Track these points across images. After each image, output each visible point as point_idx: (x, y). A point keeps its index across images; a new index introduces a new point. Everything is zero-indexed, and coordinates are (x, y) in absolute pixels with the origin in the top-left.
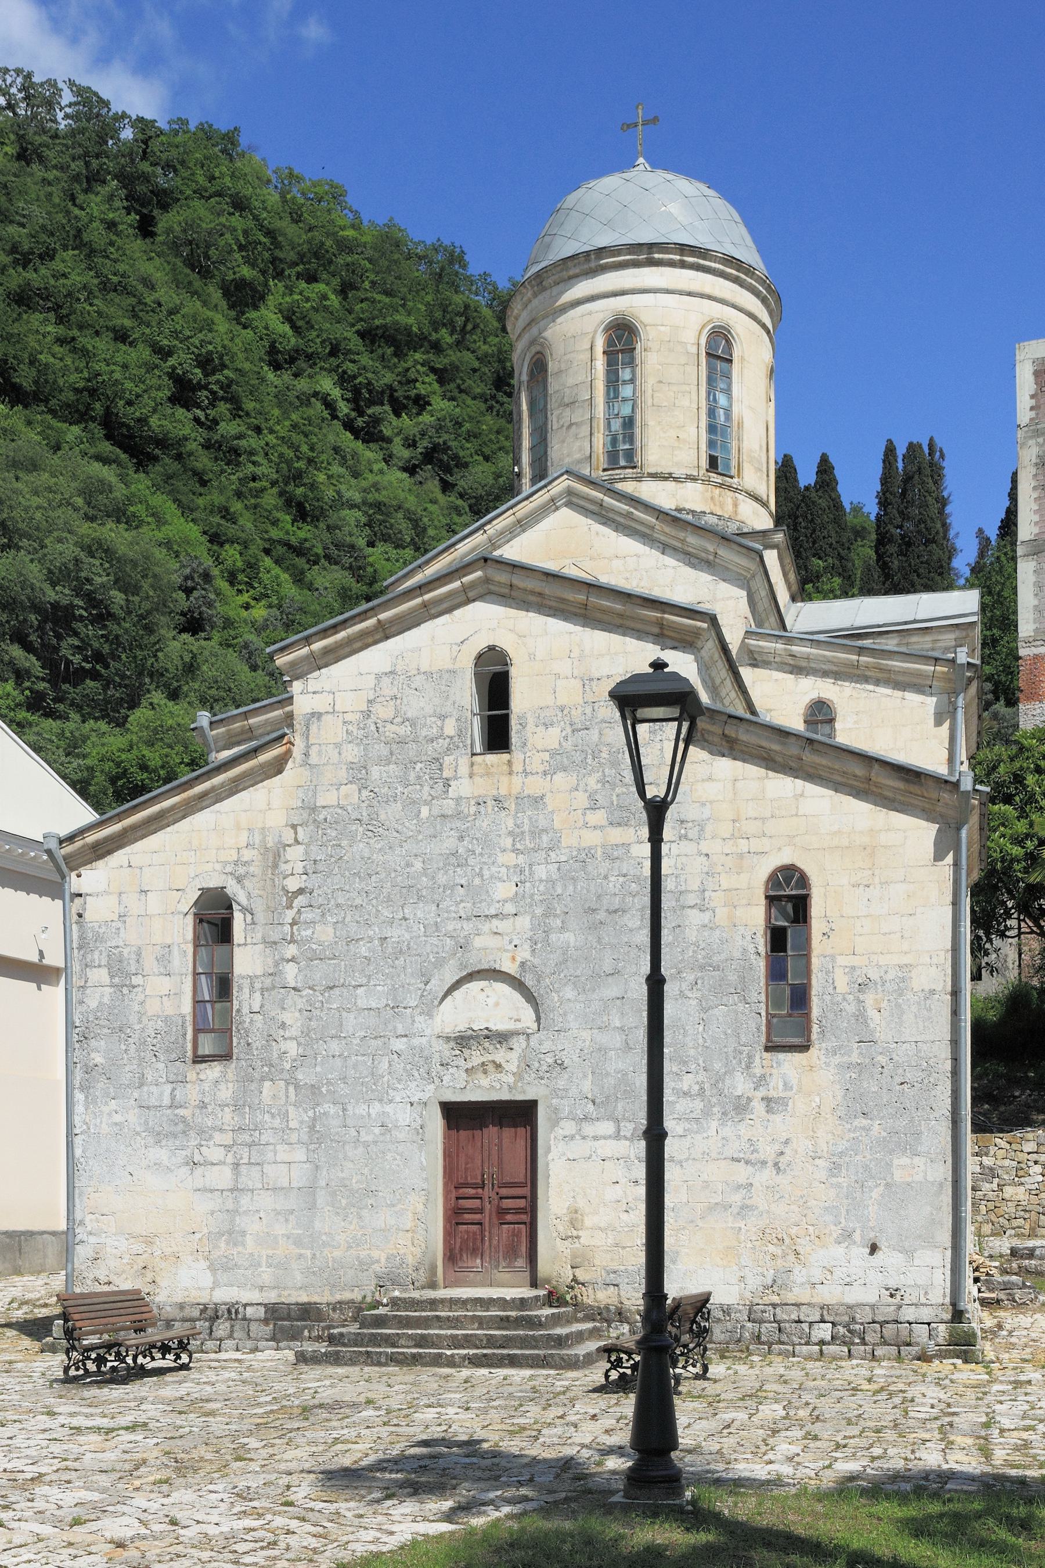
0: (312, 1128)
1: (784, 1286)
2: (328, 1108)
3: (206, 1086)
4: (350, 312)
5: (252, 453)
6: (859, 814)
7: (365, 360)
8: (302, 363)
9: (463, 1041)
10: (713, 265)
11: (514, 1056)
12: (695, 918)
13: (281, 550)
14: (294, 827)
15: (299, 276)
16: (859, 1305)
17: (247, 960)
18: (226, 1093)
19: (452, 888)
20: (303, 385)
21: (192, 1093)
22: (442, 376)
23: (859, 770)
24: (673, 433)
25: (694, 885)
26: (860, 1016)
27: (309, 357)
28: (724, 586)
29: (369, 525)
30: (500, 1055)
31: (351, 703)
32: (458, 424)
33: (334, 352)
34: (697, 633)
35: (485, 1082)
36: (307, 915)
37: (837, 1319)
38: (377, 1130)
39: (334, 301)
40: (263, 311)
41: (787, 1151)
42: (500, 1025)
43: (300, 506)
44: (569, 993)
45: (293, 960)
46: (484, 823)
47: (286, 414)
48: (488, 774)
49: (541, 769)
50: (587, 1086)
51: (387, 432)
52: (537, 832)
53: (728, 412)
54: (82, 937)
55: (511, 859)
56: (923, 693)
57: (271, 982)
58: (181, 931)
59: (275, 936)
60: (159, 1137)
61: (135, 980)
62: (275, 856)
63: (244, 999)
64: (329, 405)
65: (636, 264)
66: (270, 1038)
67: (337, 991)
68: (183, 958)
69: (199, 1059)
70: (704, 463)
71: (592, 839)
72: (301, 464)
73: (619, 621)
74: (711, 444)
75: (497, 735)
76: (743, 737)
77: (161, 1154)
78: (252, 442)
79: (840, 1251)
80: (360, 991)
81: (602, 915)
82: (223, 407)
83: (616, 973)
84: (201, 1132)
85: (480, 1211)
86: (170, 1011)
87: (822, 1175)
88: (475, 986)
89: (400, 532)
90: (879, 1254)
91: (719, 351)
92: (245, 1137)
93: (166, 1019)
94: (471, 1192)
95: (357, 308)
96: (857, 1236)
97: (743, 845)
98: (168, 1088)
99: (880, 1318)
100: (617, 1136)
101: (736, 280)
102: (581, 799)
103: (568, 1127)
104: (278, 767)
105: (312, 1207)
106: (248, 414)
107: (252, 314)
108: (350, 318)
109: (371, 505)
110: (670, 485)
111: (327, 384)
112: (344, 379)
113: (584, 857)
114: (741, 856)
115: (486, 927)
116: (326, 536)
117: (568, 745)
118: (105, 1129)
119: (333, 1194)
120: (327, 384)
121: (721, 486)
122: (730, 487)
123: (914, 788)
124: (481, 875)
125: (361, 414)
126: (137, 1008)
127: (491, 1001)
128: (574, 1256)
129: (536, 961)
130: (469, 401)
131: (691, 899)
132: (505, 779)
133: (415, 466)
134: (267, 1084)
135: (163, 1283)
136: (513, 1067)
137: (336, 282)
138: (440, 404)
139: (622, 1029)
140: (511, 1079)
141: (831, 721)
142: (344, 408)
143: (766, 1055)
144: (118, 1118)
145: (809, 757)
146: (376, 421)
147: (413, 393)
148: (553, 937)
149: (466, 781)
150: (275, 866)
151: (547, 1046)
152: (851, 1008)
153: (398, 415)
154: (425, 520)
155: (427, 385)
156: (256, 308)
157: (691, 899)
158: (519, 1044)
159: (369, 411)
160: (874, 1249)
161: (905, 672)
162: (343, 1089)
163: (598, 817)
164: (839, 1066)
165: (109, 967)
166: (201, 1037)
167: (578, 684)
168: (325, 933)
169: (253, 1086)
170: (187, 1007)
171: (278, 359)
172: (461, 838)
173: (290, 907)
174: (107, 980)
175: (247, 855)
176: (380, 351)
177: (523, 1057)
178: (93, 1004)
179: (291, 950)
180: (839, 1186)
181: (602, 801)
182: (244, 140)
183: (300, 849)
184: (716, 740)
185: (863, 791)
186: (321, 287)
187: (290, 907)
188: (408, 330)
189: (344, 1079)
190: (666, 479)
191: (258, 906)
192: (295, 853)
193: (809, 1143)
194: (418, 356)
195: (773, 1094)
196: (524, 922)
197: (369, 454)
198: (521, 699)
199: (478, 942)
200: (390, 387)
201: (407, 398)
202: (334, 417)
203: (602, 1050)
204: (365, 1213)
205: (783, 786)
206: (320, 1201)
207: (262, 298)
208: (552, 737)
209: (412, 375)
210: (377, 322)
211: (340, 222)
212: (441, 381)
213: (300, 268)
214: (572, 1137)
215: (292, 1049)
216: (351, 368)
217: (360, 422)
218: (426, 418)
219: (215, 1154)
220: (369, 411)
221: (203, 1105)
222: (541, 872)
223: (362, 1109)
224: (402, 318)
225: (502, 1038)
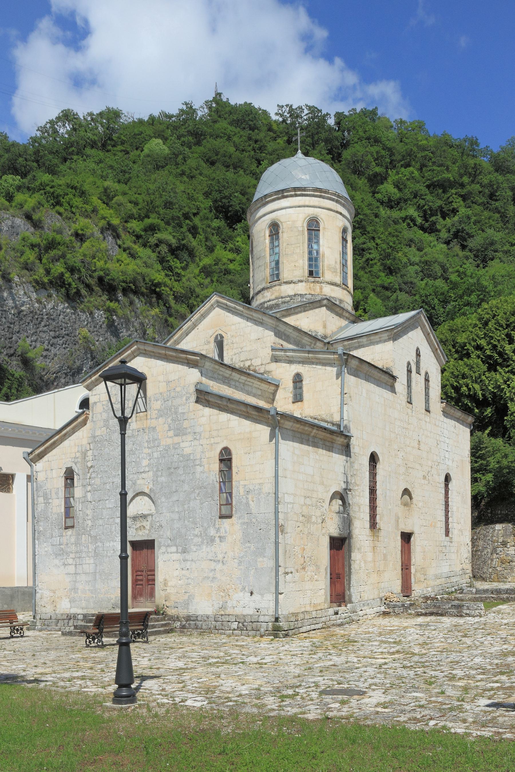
0: (95, 551)
1: (225, 608)
2: (99, 544)
3: (68, 537)
4: (423, 177)
5: (370, 249)
6: (246, 425)
7: (429, 197)
8: (402, 204)
10: (308, 193)
11: (148, 523)
12: (199, 469)
13: (379, 289)
14: (89, 444)
15: (402, 166)
16: (247, 615)
18: (73, 540)
19: (131, 463)
20: (403, 214)
21: (64, 540)
23: (243, 408)
24: (293, 264)
25: (198, 457)
26: (247, 504)
27: (406, 201)
28: (267, 331)
29: (422, 271)
30: (145, 523)
33: (415, 197)
34: (197, 361)
35: (140, 533)
36: (93, 475)
37: (240, 621)
38: (112, 552)
39: (416, 173)
40: (385, 184)
41: (226, 556)
42: (146, 512)
43: (389, 268)
44: (163, 499)
45: (90, 491)
46: (139, 438)
47: (386, 230)
48: (141, 420)
49: (155, 416)
50: (169, 534)
51: (439, 227)
52: (154, 440)
53: (318, 252)
54: (37, 487)
55: (146, 451)
56: (332, 366)
59: (85, 484)
61: (50, 501)
62: (84, 454)
64: (413, 220)
65: (278, 199)
66: (84, 520)
67: (101, 502)
69: (66, 528)
70: (307, 273)
71: (169, 441)
72: (390, 251)
73: (175, 359)
74: (310, 266)
76: (211, 399)
77: (57, 562)
79: (241, 594)
80: (107, 501)
81: (172, 470)
83: (176, 491)
84: (67, 554)
85: (142, 580)
86: (59, 512)
87: (236, 565)
88: (138, 498)
89: (436, 272)
90: (253, 595)
91: (313, 227)
92: (78, 555)
93: (58, 514)
94: (140, 573)
95: (426, 174)
96: (247, 589)
97: (212, 441)
98: (58, 538)
99: (253, 620)
100: (177, 552)
101: (320, 197)
102: (166, 427)
103: (163, 549)
105: (95, 580)
106: (369, 233)
107: (381, 187)
108: (424, 180)
109: (423, 263)
110: (292, 285)
111: (412, 211)
112: (419, 208)
113: (167, 449)
114: (212, 444)
115: (140, 476)
116: (400, 280)
117: (163, 407)
118: (43, 553)
119: (101, 575)
120: (412, 211)
121: (314, 282)
122: (318, 282)
123: (261, 414)
124: (139, 457)
125: (427, 221)
126: (50, 510)
127: (143, 503)
128: (166, 597)
129: (154, 488)
131: (198, 462)
132: (145, 421)
133: (449, 241)
134: (83, 536)
135: (58, 606)
136: (148, 527)
137: (418, 165)
138: (463, 211)
139: (178, 512)
140: (147, 532)
141: (302, 381)
142: (419, 221)
143: (220, 520)
144: (46, 549)
145: (230, 406)
146: (434, 223)
147: (451, 208)
148: (159, 479)
149: (135, 423)
150: (85, 458)
151: (158, 519)
152: (244, 501)
153: (444, 219)
154: (448, 265)
155: (458, 203)
156: (382, 183)
157: (198, 462)
158: (149, 518)
159: (431, 220)
160: (252, 593)
161: (325, 359)
162: (103, 537)
163: (171, 434)
164: (241, 523)
165: (43, 496)
166: (67, 520)
167: (165, 384)
168: (97, 481)
169: (80, 537)
170: (63, 510)
171: (391, 204)
172: (133, 444)
173: (89, 473)
174: (43, 501)
175: (78, 455)
176: (436, 192)
177: (151, 524)
178: (40, 510)
179: (89, 488)
180: (241, 569)
181: (172, 427)
182: (379, 112)
183: (91, 451)
184: (204, 401)
185: (247, 416)
186: (411, 169)
187: (89, 473)
188: (449, 180)
189: (103, 533)
190: (290, 283)
191: (80, 473)
192: (90, 453)
193: (232, 553)
194: (453, 191)
195: (222, 535)
196: (151, 474)
197: (431, 239)
199: (139, 482)
200: (441, 207)
201: (449, 210)
202: (415, 225)
203: (173, 520)
204: (109, 581)
205: (224, 416)
206: (97, 577)
207: (386, 179)
209: (451, 200)
210: (435, 179)
211: (420, 139)
212: (464, 200)
213: (402, 163)
214: (165, 553)
215: (89, 523)
216: (422, 202)
217: (427, 225)
218: (456, 218)
219: (70, 561)
220: (431, 220)
221: (67, 544)
222: (156, 455)
223: (108, 544)
224: (447, 175)
225: (144, 517)
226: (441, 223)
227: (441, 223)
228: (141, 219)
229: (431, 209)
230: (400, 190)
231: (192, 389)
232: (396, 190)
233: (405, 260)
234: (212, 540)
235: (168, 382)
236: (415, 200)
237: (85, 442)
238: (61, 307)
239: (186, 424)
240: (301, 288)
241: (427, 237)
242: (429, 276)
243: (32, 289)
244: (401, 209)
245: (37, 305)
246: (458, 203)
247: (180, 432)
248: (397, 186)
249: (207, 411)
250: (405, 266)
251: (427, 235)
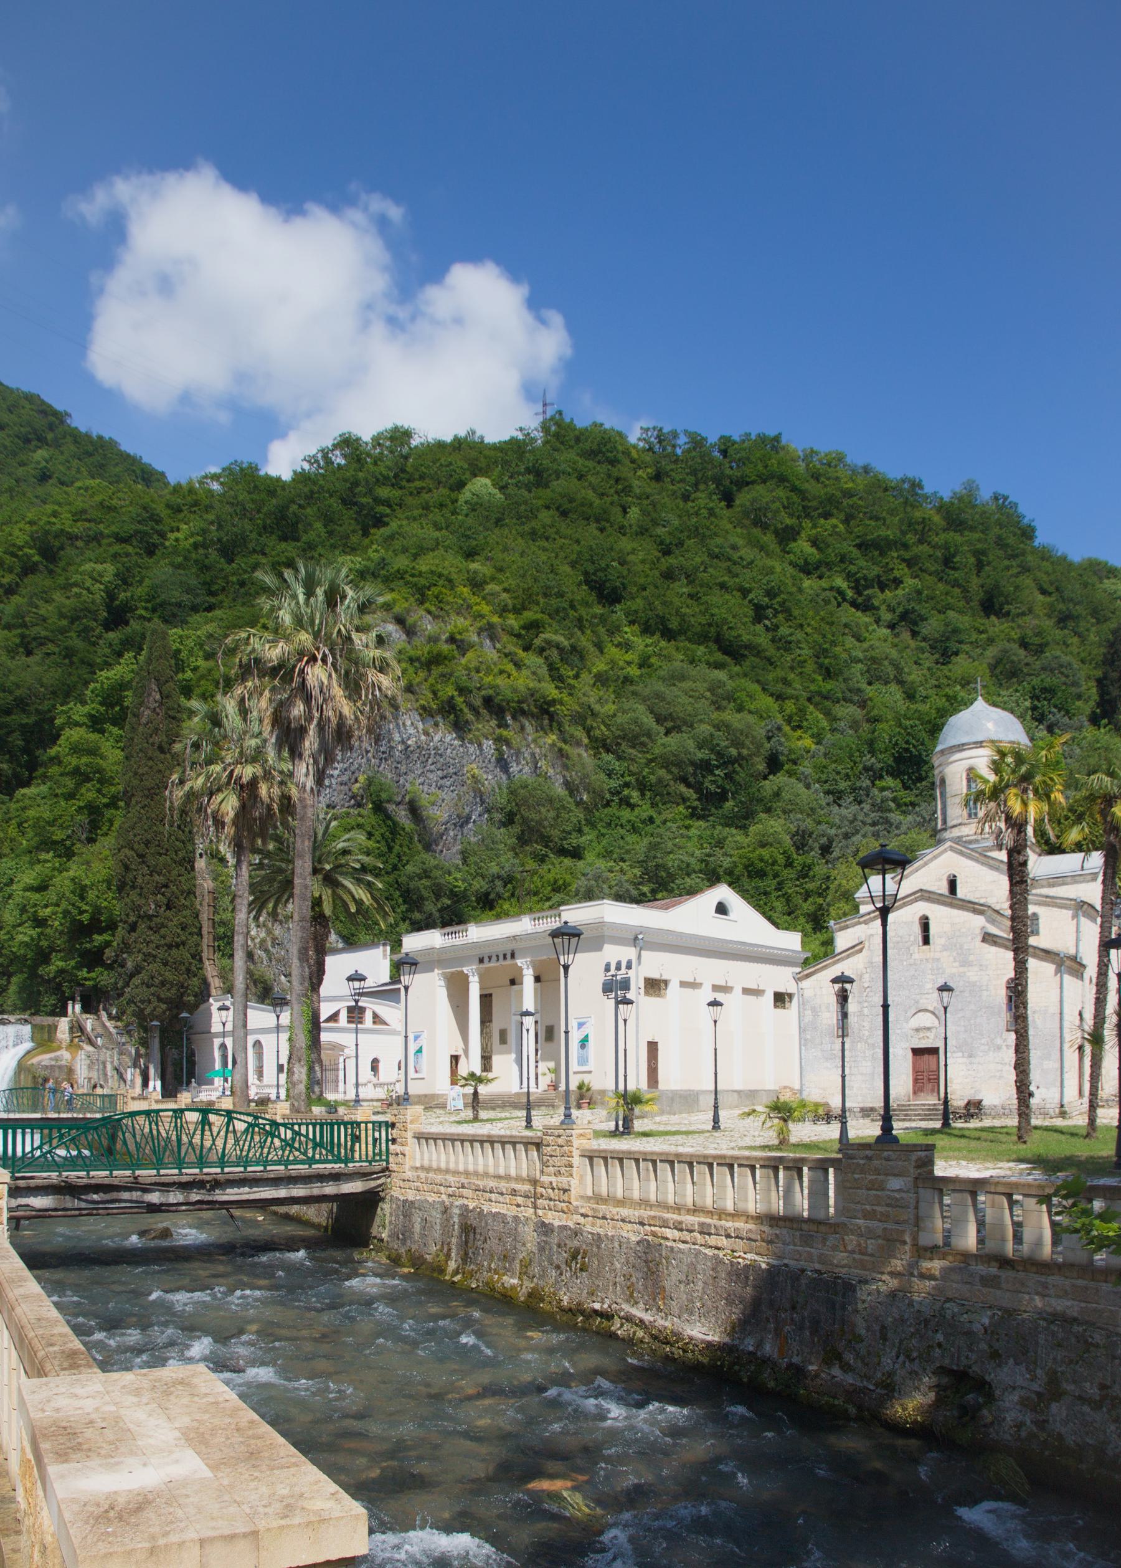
7: (862, 563)
8: (823, 569)
22: (910, 563)
27: (827, 564)
32: (919, 593)
33: (842, 561)
39: (841, 528)
47: (817, 613)
64: (840, 592)
71: (954, 970)
75: (926, 941)
78: (799, 635)
82: (781, 617)
104: (861, 950)
111: (840, 582)
112: (849, 576)
120: (840, 582)
130: (927, 577)
138: (910, 582)
142: (850, 594)
146: (869, 598)
153: (882, 591)
155: (901, 570)
156: (795, 540)
188: (886, 538)
197: (867, 619)
200: (879, 576)
202: (844, 600)
208: (943, 941)
212: (909, 566)
216: (853, 569)
218: (900, 592)
226: (879, 598)
227: (879, 598)
228: (517, 611)
229: (865, 578)
230: (819, 549)
231: (978, 931)
232: (814, 550)
233: (844, 656)
235: (953, 924)
236: (843, 566)
237: (861, 966)
238: (448, 738)
239: (971, 958)
241: (864, 619)
242: (879, 678)
243: (418, 717)
244: (820, 577)
245: (423, 738)
246: (901, 570)
247: (965, 963)
248: (814, 543)
249: (994, 949)
250: (848, 666)
251: (859, 614)
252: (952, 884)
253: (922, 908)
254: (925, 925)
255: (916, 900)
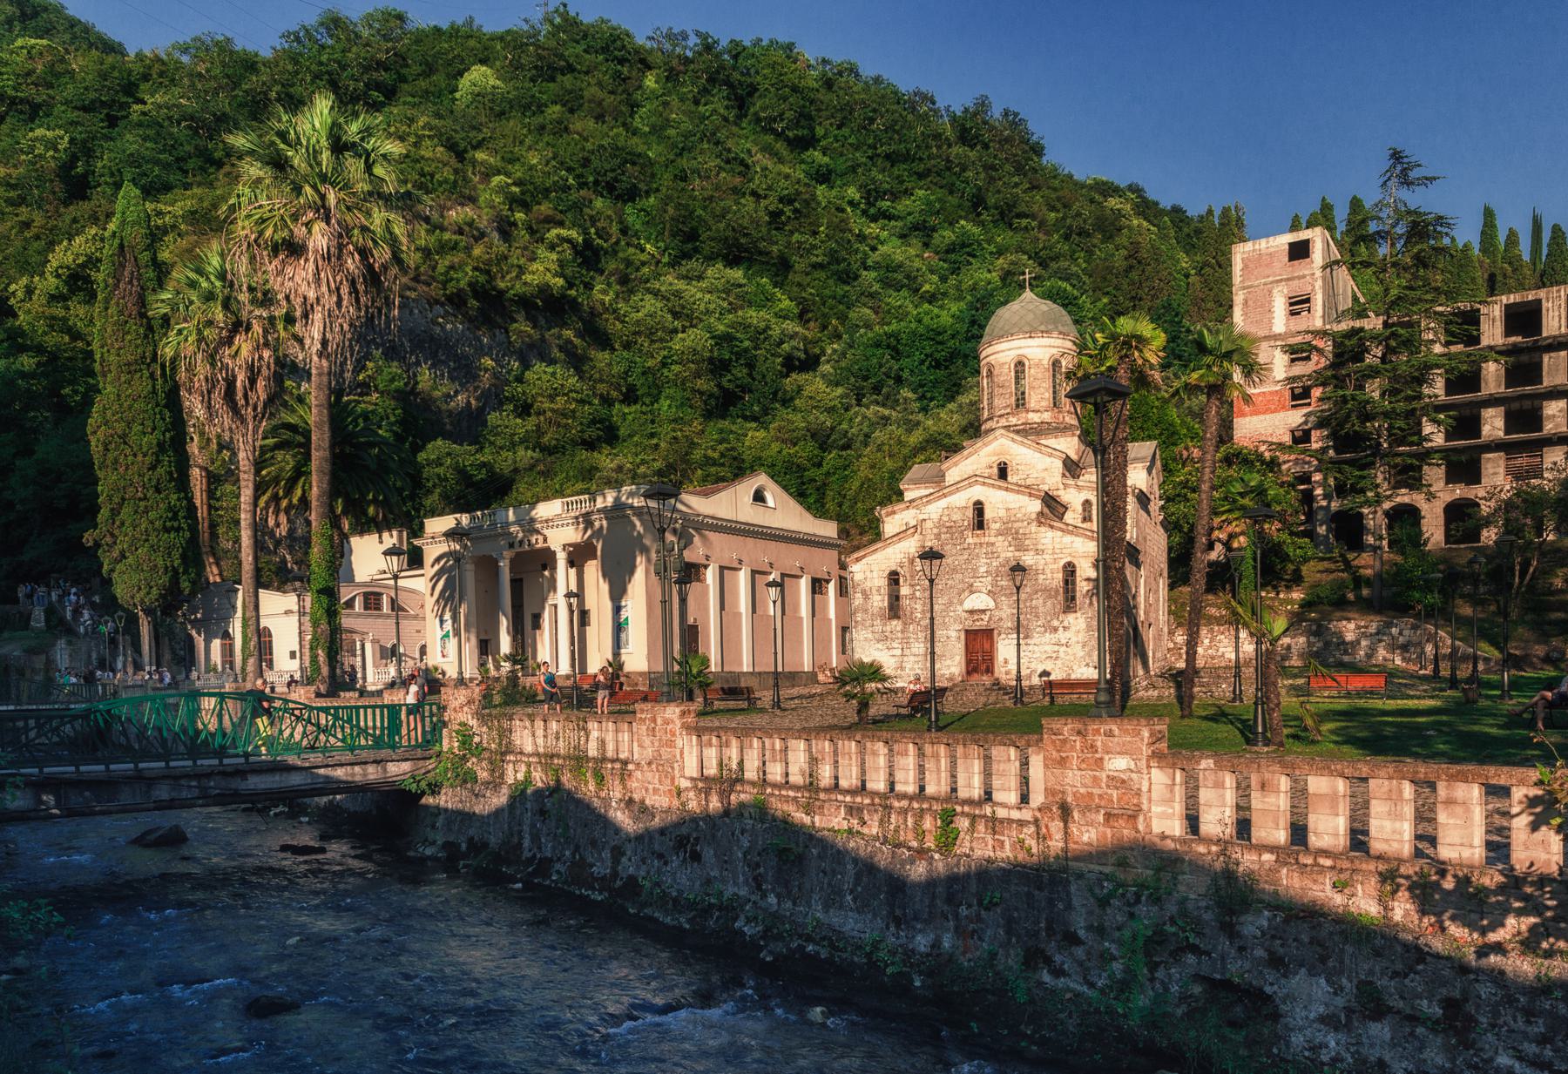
9: (971, 612)
12: (1041, 577)
17: (904, 590)
21: (888, 628)
31: (935, 517)
57: (913, 597)
58: (884, 582)
60: (879, 641)
63: (905, 602)
68: (884, 591)
77: (880, 646)
198: (988, 515)
208: (997, 526)
225: (984, 611)
234: (1056, 630)
237: (913, 550)
240: (1047, 416)
247: (1021, 548)
252: (1003, 472)
253: (978, 493)
254: (979, 508)
255: (970, 485)
